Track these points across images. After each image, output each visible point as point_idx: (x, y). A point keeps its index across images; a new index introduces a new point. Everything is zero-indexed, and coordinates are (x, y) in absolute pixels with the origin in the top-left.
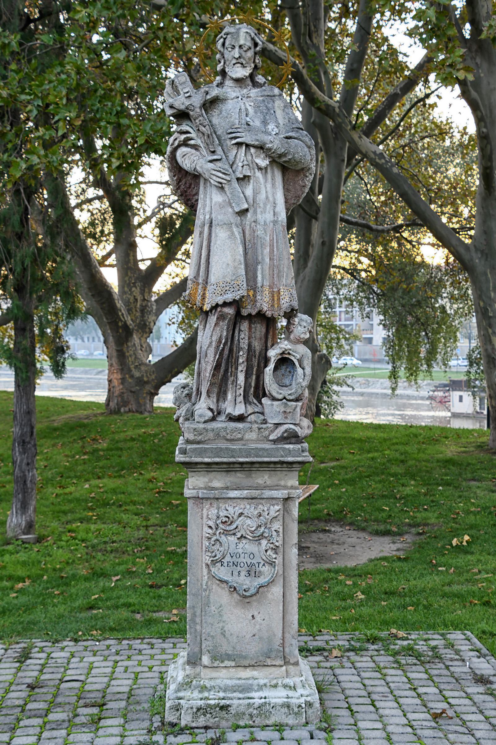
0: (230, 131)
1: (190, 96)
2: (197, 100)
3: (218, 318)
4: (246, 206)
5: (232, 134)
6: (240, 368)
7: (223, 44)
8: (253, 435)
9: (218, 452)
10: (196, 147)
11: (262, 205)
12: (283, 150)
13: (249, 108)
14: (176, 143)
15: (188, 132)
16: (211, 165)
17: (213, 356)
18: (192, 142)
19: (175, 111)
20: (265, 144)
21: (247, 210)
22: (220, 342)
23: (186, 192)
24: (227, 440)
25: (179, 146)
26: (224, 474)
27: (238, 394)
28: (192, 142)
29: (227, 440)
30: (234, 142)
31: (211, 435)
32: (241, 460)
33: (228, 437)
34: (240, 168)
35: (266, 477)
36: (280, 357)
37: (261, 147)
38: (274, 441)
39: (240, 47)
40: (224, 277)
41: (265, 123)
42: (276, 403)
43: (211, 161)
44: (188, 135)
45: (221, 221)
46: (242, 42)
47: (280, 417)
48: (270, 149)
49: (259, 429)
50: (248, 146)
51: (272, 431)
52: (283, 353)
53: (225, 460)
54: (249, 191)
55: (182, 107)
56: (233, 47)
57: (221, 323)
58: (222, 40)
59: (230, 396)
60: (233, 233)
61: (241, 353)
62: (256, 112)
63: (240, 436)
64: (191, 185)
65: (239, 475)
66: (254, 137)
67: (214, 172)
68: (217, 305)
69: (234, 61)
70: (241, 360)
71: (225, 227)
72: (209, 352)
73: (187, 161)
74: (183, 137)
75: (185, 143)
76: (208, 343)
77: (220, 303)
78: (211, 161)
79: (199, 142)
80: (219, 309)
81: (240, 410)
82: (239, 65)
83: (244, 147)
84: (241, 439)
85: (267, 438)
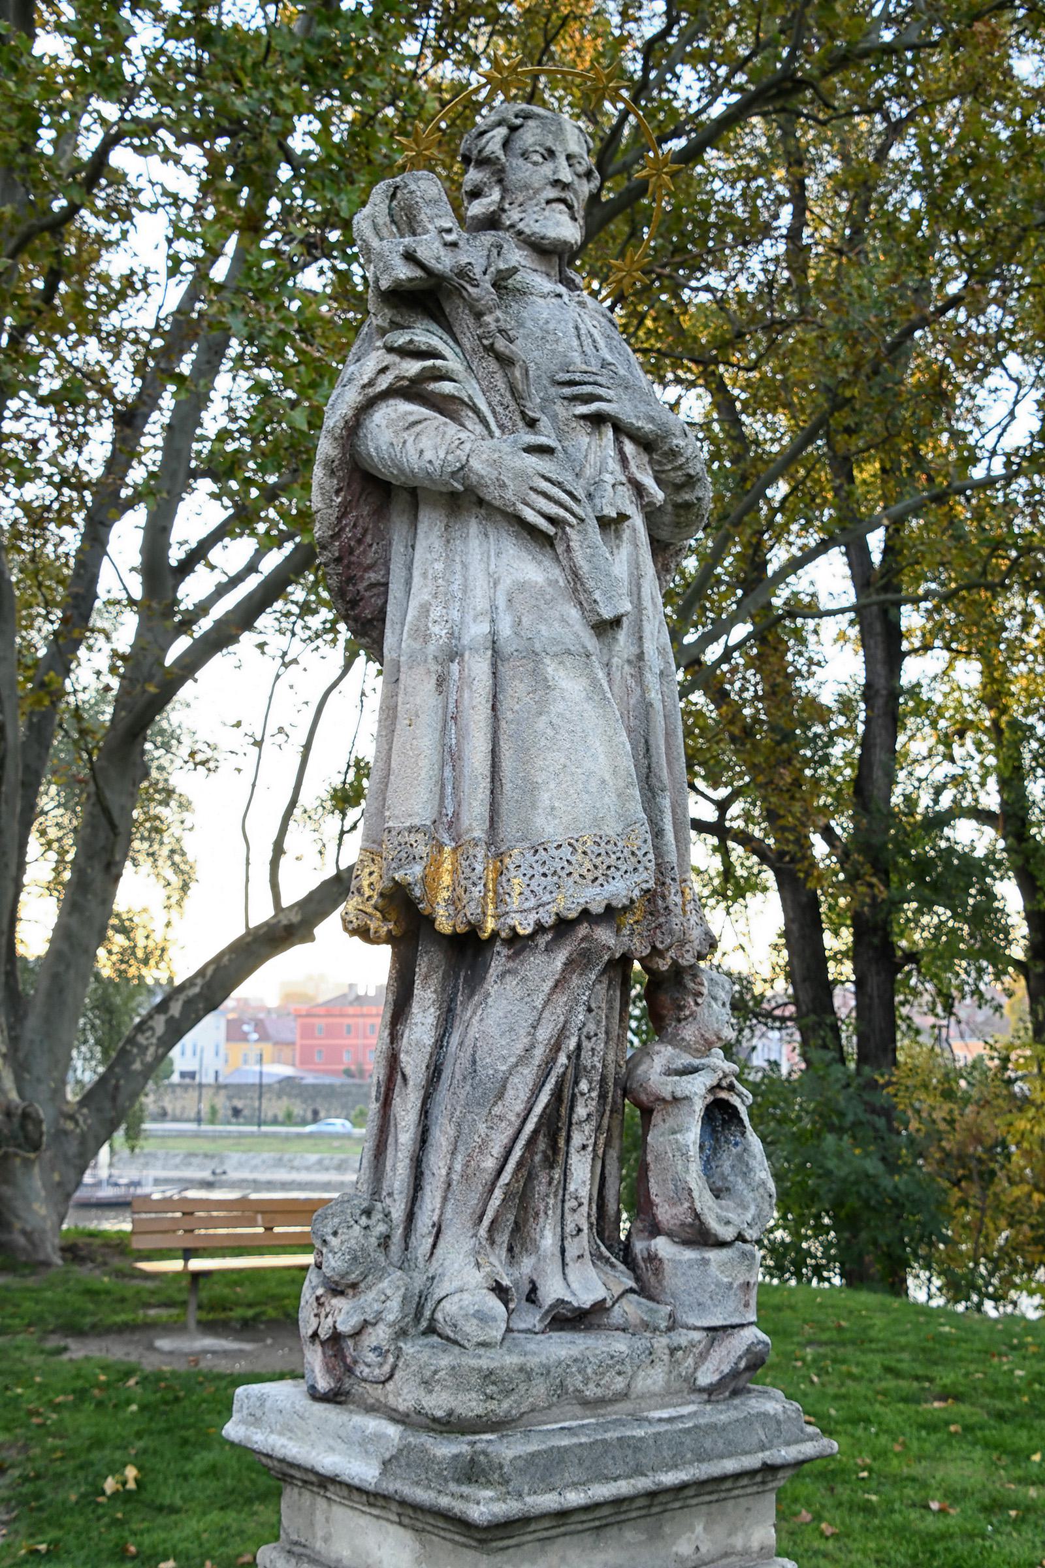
0: (567, 377)
1: (454, 245)
3: (569, 964)
6: (577, 1139)
7: (506, 144)
8: (653, 1379)
9: (594, 1460)
10: (447, 407)
13: (595, 332)
14: (384, 383)
16: (532, 460)
17: (524, 1095)
18: (447, 387)
20: (667, 434)
21: (616, 622)
22: (556, 1048)
23: (351, 551)
24: (585, 1403)
25: (390, 393)
26: (588, 1539)
27: (570, 1228)
28: (447, 387)
29: (585, 1403)
31: (540, 1390)
32: (670, 1478)
33: (591, 1391)
35: (699, 1528)
36: (710, 1098)
38: (711, 1391)
40: (597, 822)
42: (713, 1255)
44: (439, 362)
45: (555, 641)
47: (731, 1304)
48: (674, 453)
49: (673, 1351)
50: (620, 429)
51: (703, 1357)
52: (719, 1086)
53: (624, 1487)
57: (575, 980)
58: (502, 131)
59: (548, 1241)
60: (594, 682)
61: (584, 1086)
63: (620, 1384)
64: (366, 531)
65: (629, 1535)
67: (545, 486)
68: (585, 914)
69: (552, 193)
70: (581, 1111)
71: (568, 661)
72: (515, 1080)
73: (425, 443)
74: (413, 367)
75: (411, 391)
76: (519, 1048)
77: (597, 908)
78: (531, 449)
79: (470, 389)
80: (583, 930)
81: (586, 1285)
82: (562, 207)
84: (624, 1396)
85: (690, 1380)
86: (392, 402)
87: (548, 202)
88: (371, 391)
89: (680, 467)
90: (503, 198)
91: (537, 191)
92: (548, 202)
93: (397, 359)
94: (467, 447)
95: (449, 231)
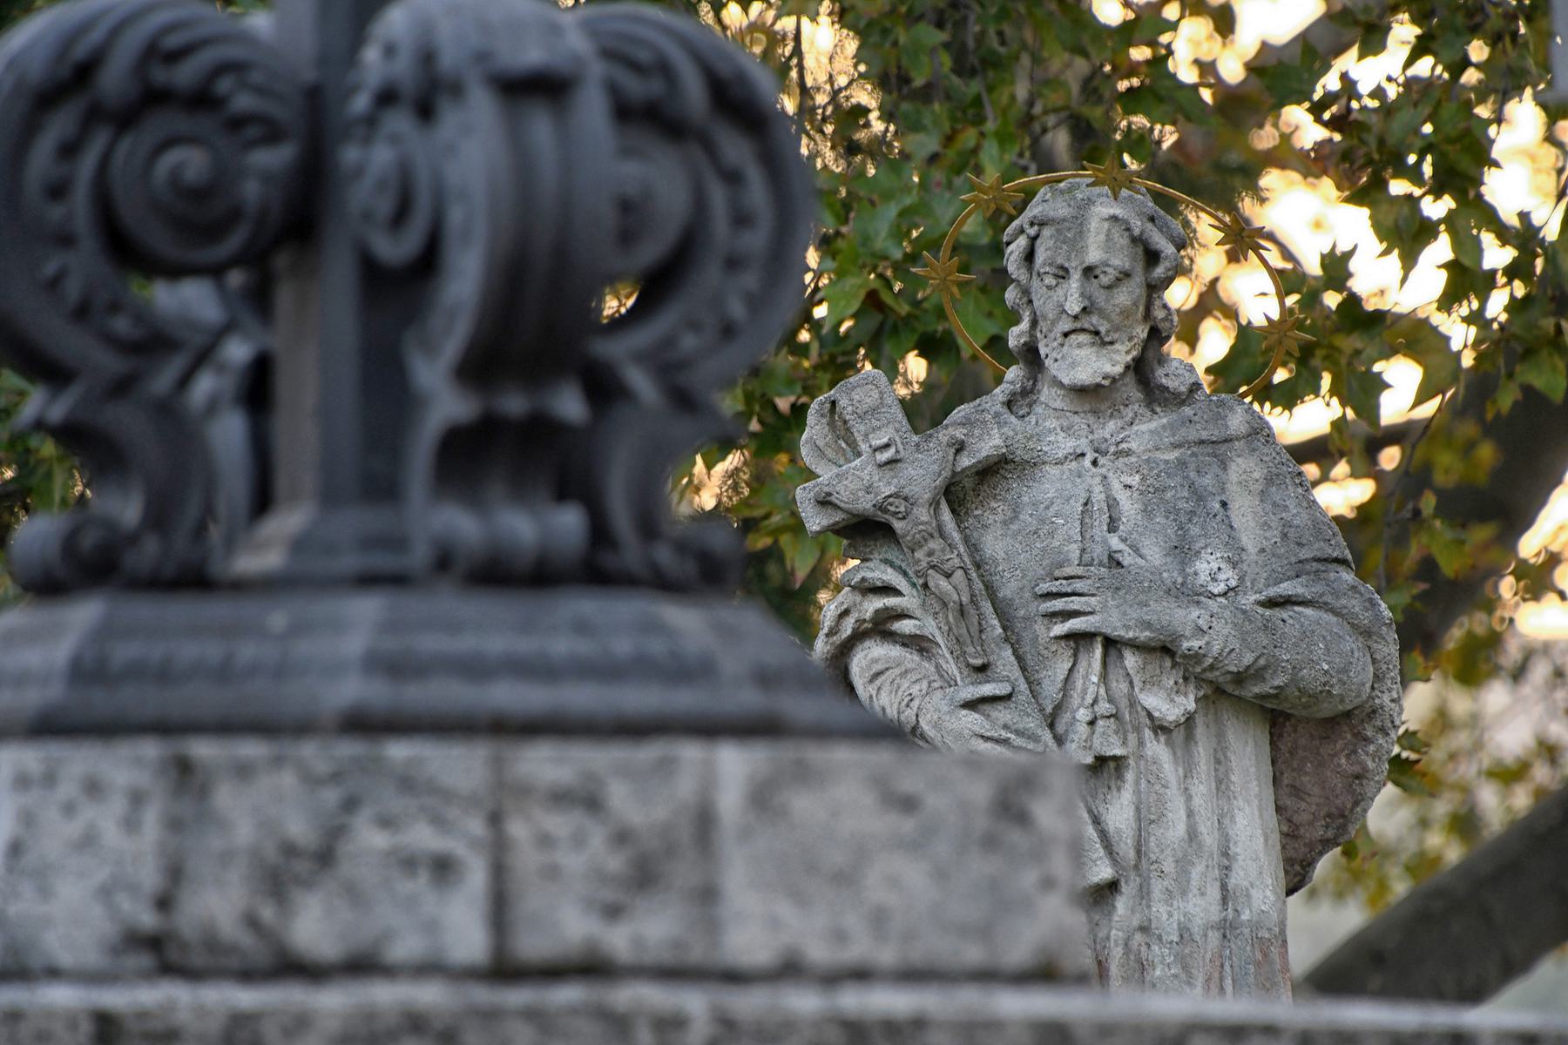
0: (1045, 587)
1: (892, 462)
2: (923, 472)
4: (1103, 872)
5: (1055, 595)
7: (1029, 256)
10: (919, 644)
11: (1169, 866)
12: (1248, 658)
13: (1123, 497)
14: (848, 628)
15: (888, 590)
16: (971, 719)
18: (905, 626)
19: (838, 517)
21: (1113, 886)
25: (858, 637)
28: (905, 626)
30: (1060, 629)
34: (1083, 729)
37: (1163, 649)
39: (1089, 272)
41: (1183, 551)
43: (971, 705)
44: (891, 601)
46: (1094, 255)
48: (1196, 657)
50: (1112, 644)
54: (1120, 813)
55: (865, 504)
56: (1063, 274)
58: (1022, 241)
62: (1147, 512)
66: (1135, 613)
69: (1066, 325)
75: (881, 627)
78: (971, 705)
79: (930, 627)
83: (1098, 652)
86: (867, 643)
87: (1066, 335)
88: (837, 639)
89: (1212, 667)
90: (1034, 323)
91: (1054, 323)
92: (1066, 335)
93: (858, 598)
94: (916, 704)
95: (887, 446)
